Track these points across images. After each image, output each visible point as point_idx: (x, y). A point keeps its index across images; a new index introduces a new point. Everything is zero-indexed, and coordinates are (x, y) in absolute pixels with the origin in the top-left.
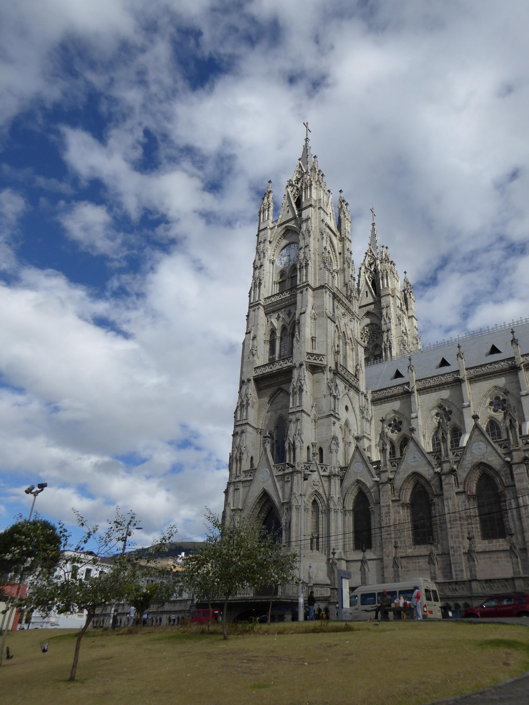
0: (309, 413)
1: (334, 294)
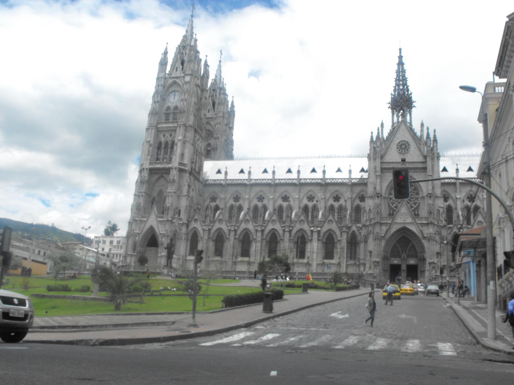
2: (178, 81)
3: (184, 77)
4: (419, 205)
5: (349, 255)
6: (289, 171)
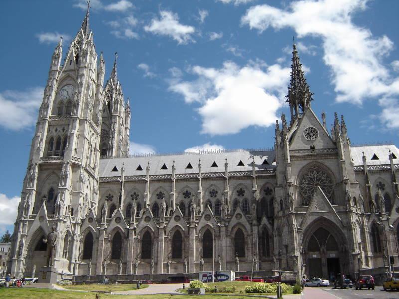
1: (90, 123)
2: (71, 74)
3: (78, 70)
4: (333, 193)
5: (262, 251)
6: (189, 167)
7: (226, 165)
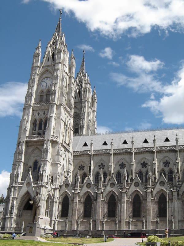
0: (49, 161)
1: (65, 108)
2: (49, 68)
3: (54, 65)
7: (177, 140)
